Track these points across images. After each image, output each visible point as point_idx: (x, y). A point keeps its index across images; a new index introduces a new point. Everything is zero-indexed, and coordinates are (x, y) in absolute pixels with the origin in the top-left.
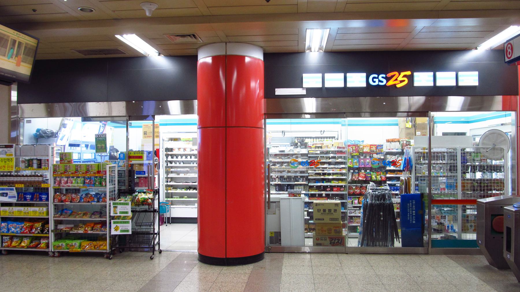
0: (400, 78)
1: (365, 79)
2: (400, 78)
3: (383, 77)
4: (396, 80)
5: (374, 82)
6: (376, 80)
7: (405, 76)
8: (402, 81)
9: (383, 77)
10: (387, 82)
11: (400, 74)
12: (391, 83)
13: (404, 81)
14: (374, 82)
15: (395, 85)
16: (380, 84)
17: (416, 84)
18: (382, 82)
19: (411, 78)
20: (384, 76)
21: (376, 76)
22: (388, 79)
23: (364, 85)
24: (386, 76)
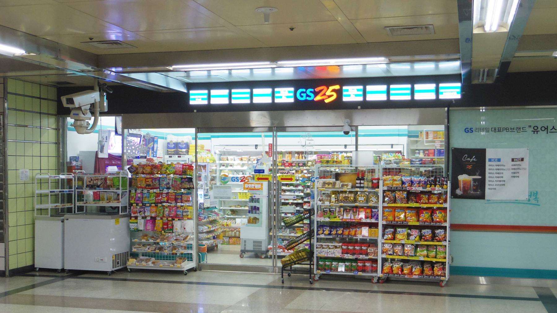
0: (328, 93)
1: (292, 94)
2: (328, 93)
3: (311, 92)
5: (302, 97)
6: (304, 95)
7: (334, 90)
8: (329, 96)
9: (311, 92)
10: (315, 96)
11: (328, 88)
12: (318, 98)
13: (332, 96)
14: (302, 97)
15: (323, 100)
16: (308, 98)
17: (345, 99)
18: (310, 97)
19: (339, 93)
20: (312, 90)
21: (304, 90)
22: (316, 94)
23: (292, 100)
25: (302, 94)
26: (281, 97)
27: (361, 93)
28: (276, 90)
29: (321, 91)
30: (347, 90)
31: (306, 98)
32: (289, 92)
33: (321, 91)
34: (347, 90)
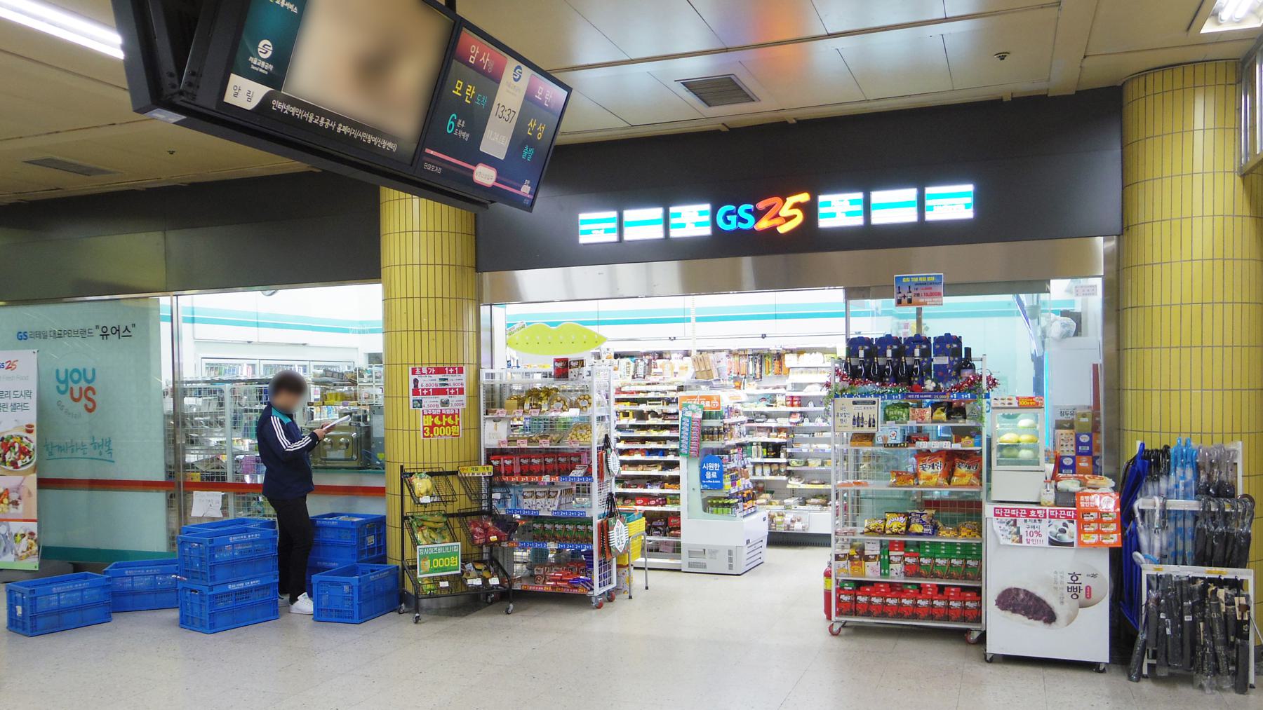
1: (707, 218)
2: (785, 211)
3: (748, 211)
4: (777, 216)
5: (728, 222)
6: (733, 218)
8: (788, 219)
9: (748, 211)
10: (756, 222)
11: (784, 201)
12: (764, 224)
13: (793, 217)
14: (728, 222)
16: (742, 226)
17: (823, 223)
18: (745, 221)
19: (810, 210)
20: (750, 207)
21: (731, 208)
22: (758, 215)
23: (707, 231)
24: (755, 208)
25: (729, 218)
26: (683, 226)
27: (860, 208)
28: (673, 210)
29: (768, 209)
30: (828, 204)
31: (737, 224)
32: (701, 213)
33: (768, 209)
34: (828, 204)
